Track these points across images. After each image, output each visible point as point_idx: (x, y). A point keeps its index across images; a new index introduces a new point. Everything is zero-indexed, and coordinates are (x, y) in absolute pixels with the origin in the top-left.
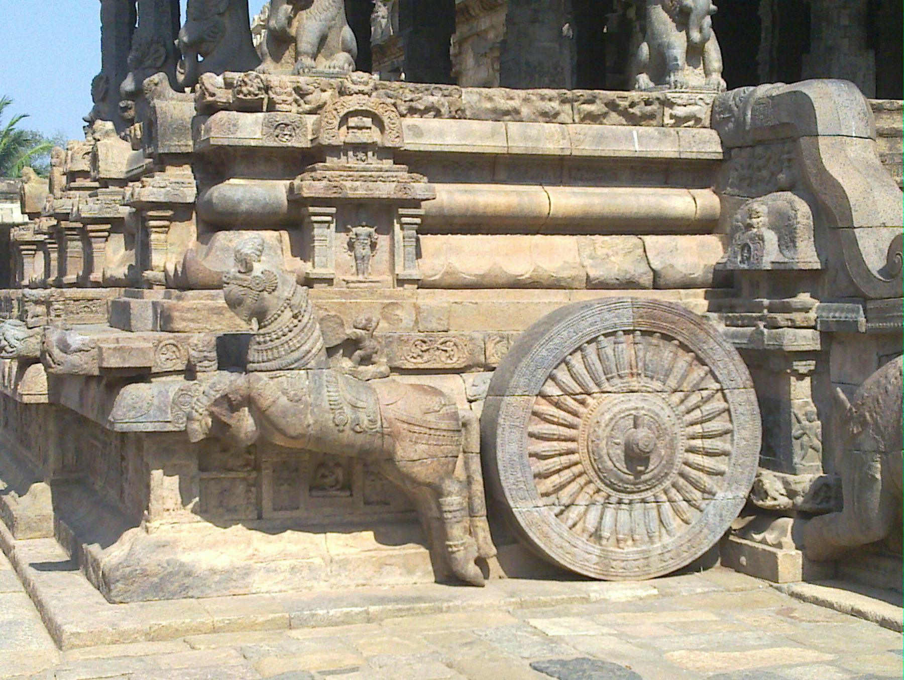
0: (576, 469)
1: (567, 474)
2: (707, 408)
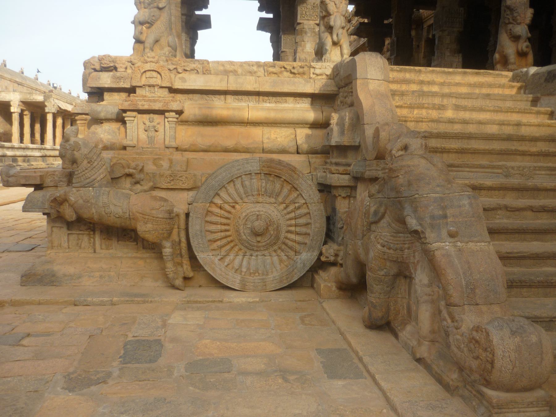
0: (229, 239)
1: (224, 241)
2: (298, 212)
